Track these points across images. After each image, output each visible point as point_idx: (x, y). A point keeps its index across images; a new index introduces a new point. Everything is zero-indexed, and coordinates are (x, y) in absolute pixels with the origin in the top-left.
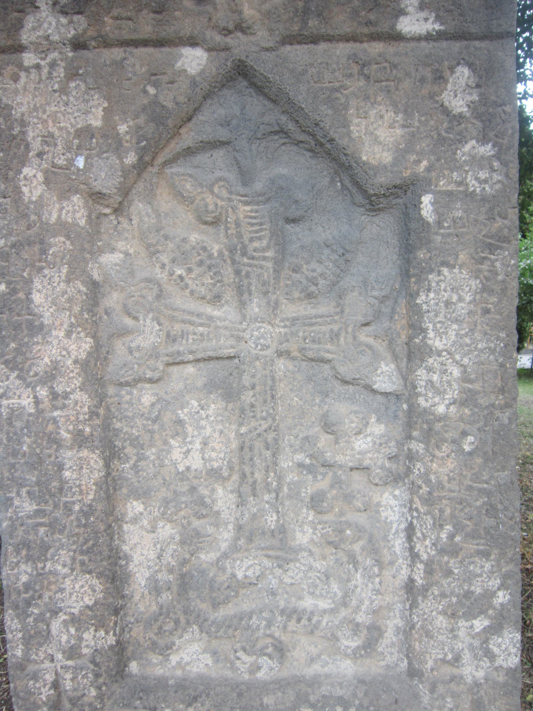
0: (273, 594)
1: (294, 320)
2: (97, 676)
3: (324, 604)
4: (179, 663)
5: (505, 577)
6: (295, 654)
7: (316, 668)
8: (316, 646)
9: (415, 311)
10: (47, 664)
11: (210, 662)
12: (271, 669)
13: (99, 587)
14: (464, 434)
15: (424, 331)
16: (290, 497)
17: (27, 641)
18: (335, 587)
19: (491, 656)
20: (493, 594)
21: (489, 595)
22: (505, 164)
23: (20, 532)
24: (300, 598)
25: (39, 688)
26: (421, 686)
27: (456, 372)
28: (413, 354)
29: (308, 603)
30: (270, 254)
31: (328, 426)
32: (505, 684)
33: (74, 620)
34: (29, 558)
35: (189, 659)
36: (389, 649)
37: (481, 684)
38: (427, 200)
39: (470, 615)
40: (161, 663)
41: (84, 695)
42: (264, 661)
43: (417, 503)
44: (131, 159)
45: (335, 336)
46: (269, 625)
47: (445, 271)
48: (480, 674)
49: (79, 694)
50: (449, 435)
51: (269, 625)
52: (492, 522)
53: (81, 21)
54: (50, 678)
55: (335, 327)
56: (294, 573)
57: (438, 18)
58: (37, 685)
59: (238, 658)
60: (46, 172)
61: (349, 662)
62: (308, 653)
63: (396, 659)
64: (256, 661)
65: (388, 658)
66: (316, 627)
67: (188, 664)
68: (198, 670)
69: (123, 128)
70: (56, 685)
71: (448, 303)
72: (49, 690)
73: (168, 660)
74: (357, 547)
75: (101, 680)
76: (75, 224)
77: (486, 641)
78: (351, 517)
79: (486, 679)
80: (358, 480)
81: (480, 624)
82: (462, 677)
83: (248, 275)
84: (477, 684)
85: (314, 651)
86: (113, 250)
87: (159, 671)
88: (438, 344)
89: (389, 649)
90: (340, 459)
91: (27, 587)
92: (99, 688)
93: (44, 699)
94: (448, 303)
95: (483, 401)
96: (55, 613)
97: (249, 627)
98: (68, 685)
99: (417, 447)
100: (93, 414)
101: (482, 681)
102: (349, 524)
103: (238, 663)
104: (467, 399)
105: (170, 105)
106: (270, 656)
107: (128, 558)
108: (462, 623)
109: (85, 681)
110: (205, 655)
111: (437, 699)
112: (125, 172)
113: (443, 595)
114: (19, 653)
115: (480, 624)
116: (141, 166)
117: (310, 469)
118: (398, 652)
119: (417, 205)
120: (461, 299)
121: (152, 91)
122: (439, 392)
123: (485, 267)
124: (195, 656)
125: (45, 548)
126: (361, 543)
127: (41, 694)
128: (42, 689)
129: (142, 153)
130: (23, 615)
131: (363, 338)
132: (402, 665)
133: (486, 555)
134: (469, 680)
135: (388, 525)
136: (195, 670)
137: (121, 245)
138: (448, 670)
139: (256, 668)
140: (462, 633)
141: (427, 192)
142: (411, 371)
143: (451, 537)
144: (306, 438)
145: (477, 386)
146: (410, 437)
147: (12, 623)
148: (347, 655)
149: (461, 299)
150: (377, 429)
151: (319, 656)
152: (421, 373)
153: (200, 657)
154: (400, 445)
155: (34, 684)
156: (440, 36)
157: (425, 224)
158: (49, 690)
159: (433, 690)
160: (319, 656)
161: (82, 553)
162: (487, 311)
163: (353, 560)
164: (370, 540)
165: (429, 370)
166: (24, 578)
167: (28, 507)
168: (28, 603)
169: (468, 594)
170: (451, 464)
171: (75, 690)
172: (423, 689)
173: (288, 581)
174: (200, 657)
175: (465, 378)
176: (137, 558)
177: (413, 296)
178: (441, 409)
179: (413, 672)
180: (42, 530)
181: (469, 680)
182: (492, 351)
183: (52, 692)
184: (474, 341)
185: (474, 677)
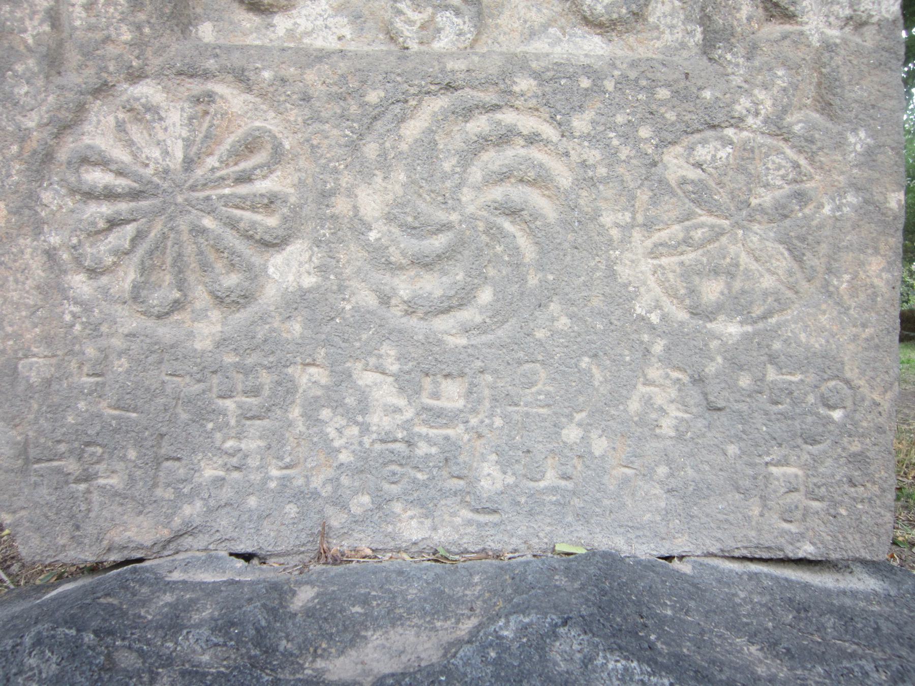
4: (291, 33)
6: (503, 20)
8: (539, 10)
11: (347, 32)
12: (460, 34)
25: (22, 20)
26: (729, 57)
35: (310, 26)
36: (669, 19)
37: (836, 45)
40: (257, 29)
41: (107, 39)
42: (444, 19)
49: (99, 36)
58: (18, 14)
59: (400, 12)
61: (597, 39)
62: (525, 22)
63: (680, 36)
64: (432, 19)
65: (667, 36)
67: (308, 34)
68: (324, 44)
72: (40, 25)
73: (270, 25)
75: (142, 17)
82: (802, 33)
87: (253, 40)
89: (669, 19)
92: (139, 28)
93: (30, 41)
101: (838, 41)
103: (399, 24)
106: (458, 12)
109: (112, 10)
110: (338, 19)
111: (760, 70)
118: (683, 24)
124: (320, 22)
127: (25, 31)
128: (27, 23)
132: (691, 43)
134: (815, 41)
136: (319, 43)
139: (430, 30)
151: (545, 27)
153: (331, 22)
155: (11, 12)
158: (40, 25)
160: (545, 27)
171: (91, 28)
174: (331, 22)
181: (815, 41)
183: (46, 28)
185: (822, 33)
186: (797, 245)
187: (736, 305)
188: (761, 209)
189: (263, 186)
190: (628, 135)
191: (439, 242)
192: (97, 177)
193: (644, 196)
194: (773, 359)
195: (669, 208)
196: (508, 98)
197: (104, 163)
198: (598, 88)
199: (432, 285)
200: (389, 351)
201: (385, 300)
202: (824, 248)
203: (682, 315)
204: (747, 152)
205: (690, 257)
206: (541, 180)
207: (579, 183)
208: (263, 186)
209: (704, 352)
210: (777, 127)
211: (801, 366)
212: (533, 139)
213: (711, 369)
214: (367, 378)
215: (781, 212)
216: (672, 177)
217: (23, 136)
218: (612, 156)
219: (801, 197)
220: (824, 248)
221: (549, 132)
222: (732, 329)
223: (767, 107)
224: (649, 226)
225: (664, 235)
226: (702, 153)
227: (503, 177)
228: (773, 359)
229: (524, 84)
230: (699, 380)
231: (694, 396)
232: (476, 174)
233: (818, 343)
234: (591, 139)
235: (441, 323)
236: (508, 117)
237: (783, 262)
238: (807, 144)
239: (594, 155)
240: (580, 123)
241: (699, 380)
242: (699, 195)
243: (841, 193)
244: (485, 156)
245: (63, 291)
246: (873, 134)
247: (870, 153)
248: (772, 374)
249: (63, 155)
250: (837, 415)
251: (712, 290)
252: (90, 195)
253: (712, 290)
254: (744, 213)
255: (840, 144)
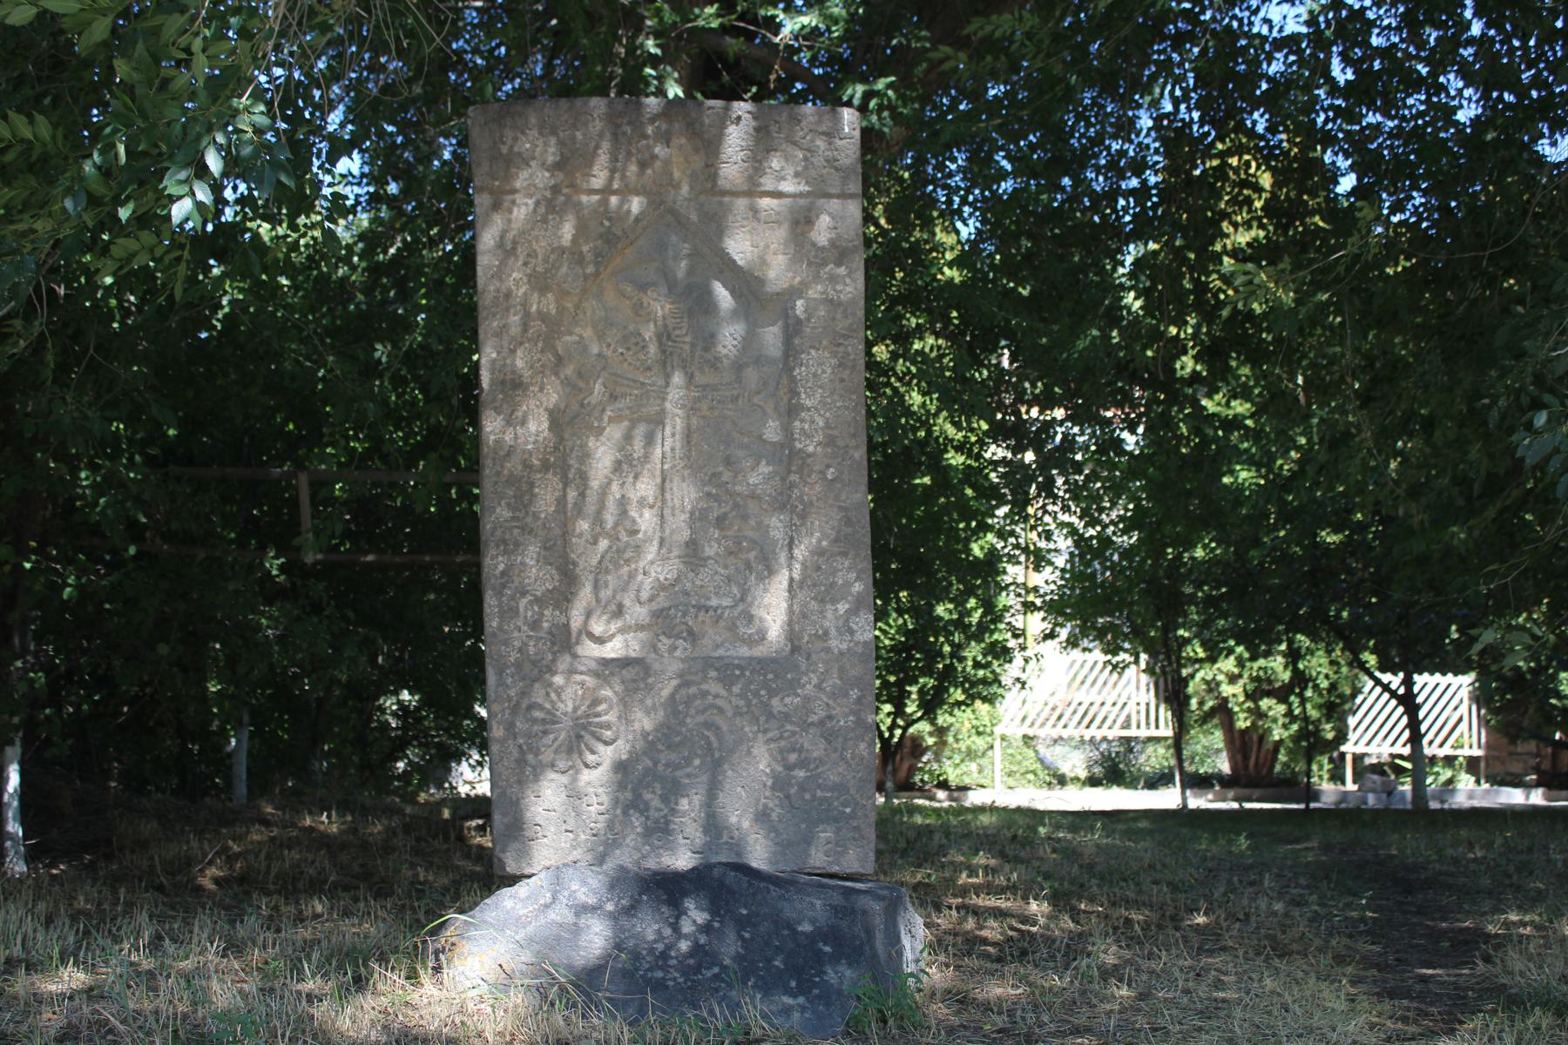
0: (687, 594)
1: (704, 387)
2: (553, 644)
3: (726, 602)
5: (860, 572)
7: (721, 652)
9: (793, 380)
10: (516, 634)
13: (557, 577)
14: (828, 466)
15: (798, 394)
16: (700, 519)
17: (502, 614)
18: (735, 590)
19: (852, 632)
20: (851, 585)
21: (848, 584)
22: (854, 281)
23: (499, 533)
24: (709, 599)
27: (821, 424)
28: (792, 411)
29: (714, 602)
30: (688, 339)
31: (728, 462)
32: (862, 654)
33: (537, 600)
34: (505, 552)
38: (799, 303)
39: (834, 601)
43: (796, 520)
44: (590, 269)
45: (735, 399)
46: (684, 616)
47: (813, 352)
48: (844, 646)
50: (817, 468)
51: (684, 616)
52: (850, 530)
53: (560, 176)
54: (517, 644)
55: (735, 392)
56: (704, 576)
57: (807, 183)
60: (530, 276)
66: (720, 617)
69: (585, 249)
70: (520, 650)
71: (815, 375)
74: (752, 555)
76: (548, 313)
77: (847, 620)
78: (750, 534)
79: (849, 649)
80: (752, 506)
81: (842, 607)
83: (671, 354)
84: (841, 654)
85: (719, 640)
86: (571, 334)
88: (808, 403)
90: (738, 488)
91: (503, 573)
94: (815, 375)
95: (841, 443)
96: (524, 594)
97: (668, 616)
98: (532, 650)
99: (794, 477)
100: (556, 448)
102: (746, 538)
104: (830, 442)
105: (619, 233)
107: (575, 564)
108: (829, 606)
112: (586, 278)
113: (815, 585)
114: (495, 624)
115: (842, 607)
116: (597, 274)
117: (716, 498)
119: (793, 308)
120: (824, 372)
121: (607, 223)
122: (808, 436)
123: (841, 349)
125: (517, 544)
126: (754, 553)
129: (597, 264)
130: (499, 594)
131: (756, 400)
133: (844, 554)
135: (775, 542)
137: (578, 330)
138: (819, 645)
140: (829, 614)
141: (800, 298)
142: (790, 424)
143: (819, 541)
144: (714, 474)
145: (835, 433)
146: (790, 472)
147: (490, 602)
148: (744, 641)
149: (824, 372)
150: (764, 469)
152: (797, 423)
154: (783, 480)
156: (808, 194)
157: (799, 321)
159: (808, 659)
161: (546, 549)
162: (842, 380)
163: (748, 566)
164: (762, 550)
165: (802, 421)
166: (501, 567)
167: (507, 514)
168: (504, 586)
169: (833, 584)
170: (818, 488)
172: (801, 659)
173: (699, 583)
175: (827, 426)
176: (582, 564)
177: (792, 370)
178: (811, 449)
179: (795, 649)
180: (516, 531)
182: (847, 408)
184: (834, 401)
186: (829, 736)
187: (803, 764)
188: (812, 724)
189: (604, 718)
190: (756, 694)
191: (678, 739)
192: (538, 714)
193: (762, 719)
194: (819, 786)
195: (773, 724)
196: (705, 679)
197: (541, 708)
198: (743, 674)
199: (673, 757)
200: (658, 785)
201: (655, 764)
202: (840, 739)
203: (780, 769)
204: (807, 699)
205: (783, 743)
206: (721, 710)
207: (735, 715)
208: (604, 718)
209: (790, 784)
210: (819, 687)
211: (832, 789)
212: (716, 696)
213: (793, 791)
214: (648, 796)
215: (821, 723)
216: (775, 711)
217: (510, 699)
218: (749, 704)
219: (830, 717)
220: (840, 739)
221: (723, 693)
222: (801, 774)
223: (815, 680)
224: (765, 731)
225: (770, 735)
226: (788, 700)
227: (703, 712)
228: (819, 786)
229: (713, 674)
230: (788, 797)
231: (786, 802)
232: (693, 711)
233: (837, 779)
234: (741, 696)
235: (678, 773)
236: (705, 687)
237: (822, 744)
238: (833, 696)
239: (742, 703)
240: (736, 689)
241: (788, 797)
242: (786, 717)
243: (847, 716)
244: (698, 702)
245: (525, 762)
246: (860, 690)
247: (859, 700)
248: (819, 793)
249: (524, 706)
250: (848, 810)
251: (793, 757)
252: (535, 721)
253: (793, 757)
254: (805, 726)
255: (846, 695)
